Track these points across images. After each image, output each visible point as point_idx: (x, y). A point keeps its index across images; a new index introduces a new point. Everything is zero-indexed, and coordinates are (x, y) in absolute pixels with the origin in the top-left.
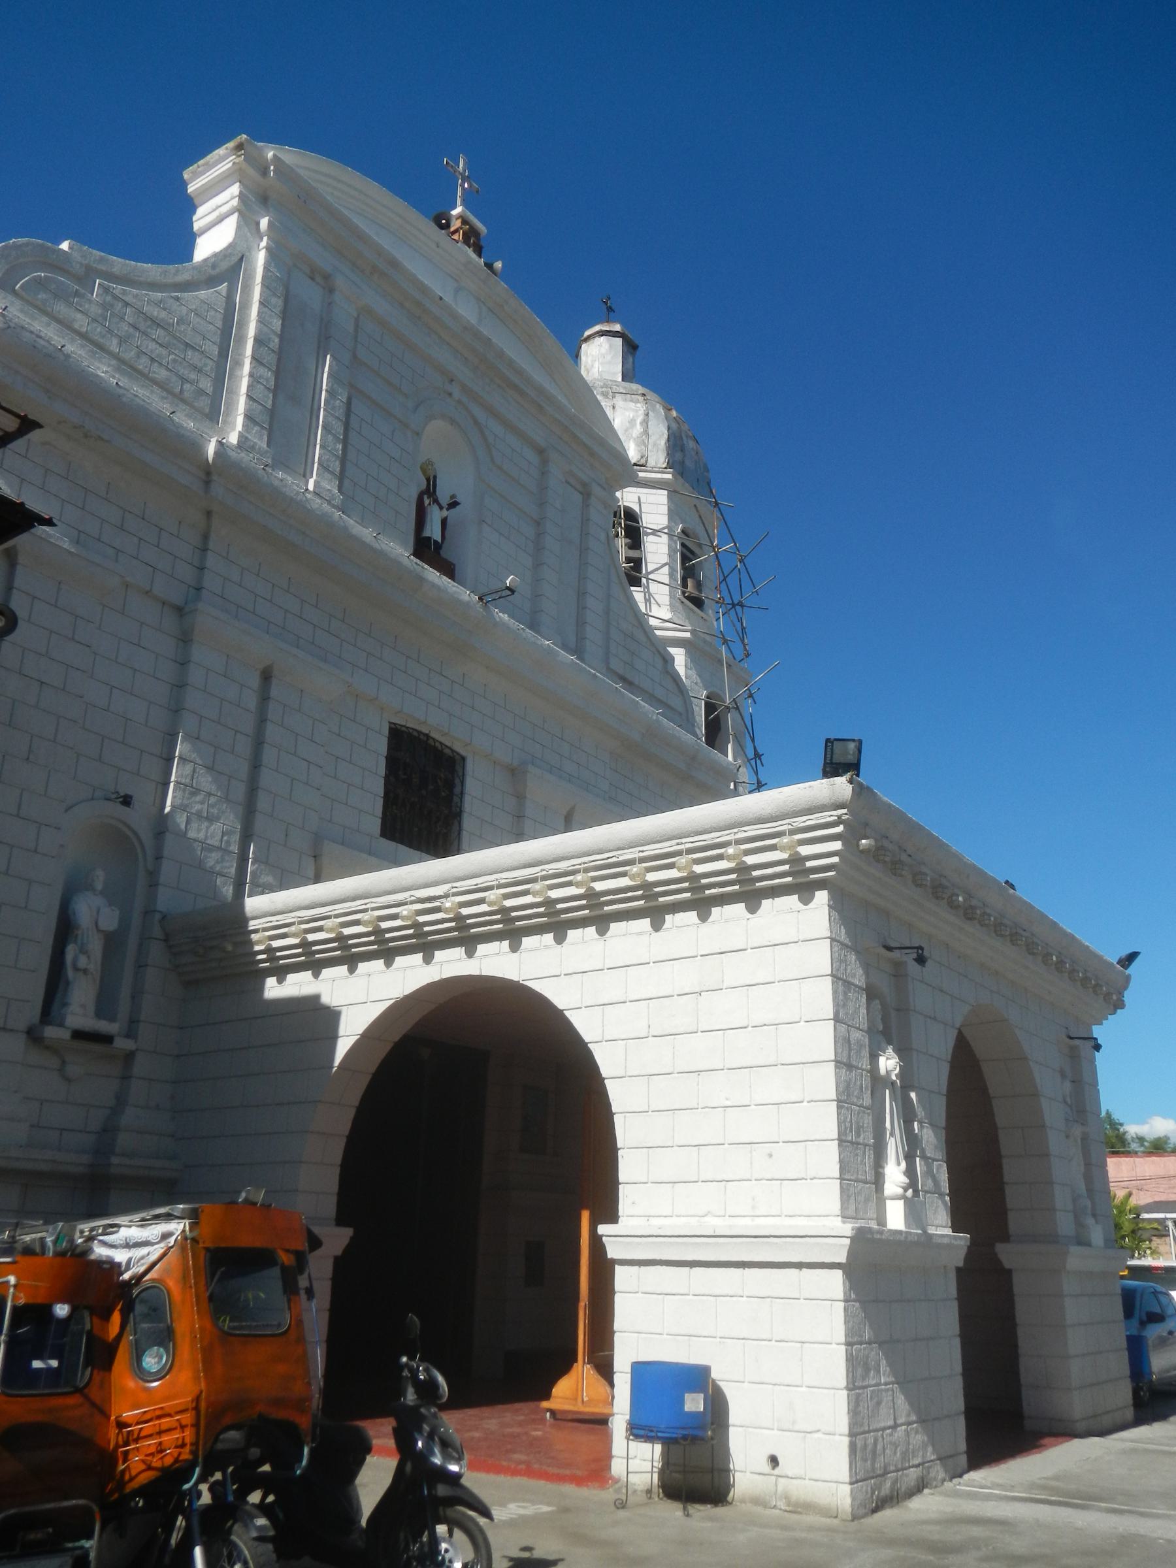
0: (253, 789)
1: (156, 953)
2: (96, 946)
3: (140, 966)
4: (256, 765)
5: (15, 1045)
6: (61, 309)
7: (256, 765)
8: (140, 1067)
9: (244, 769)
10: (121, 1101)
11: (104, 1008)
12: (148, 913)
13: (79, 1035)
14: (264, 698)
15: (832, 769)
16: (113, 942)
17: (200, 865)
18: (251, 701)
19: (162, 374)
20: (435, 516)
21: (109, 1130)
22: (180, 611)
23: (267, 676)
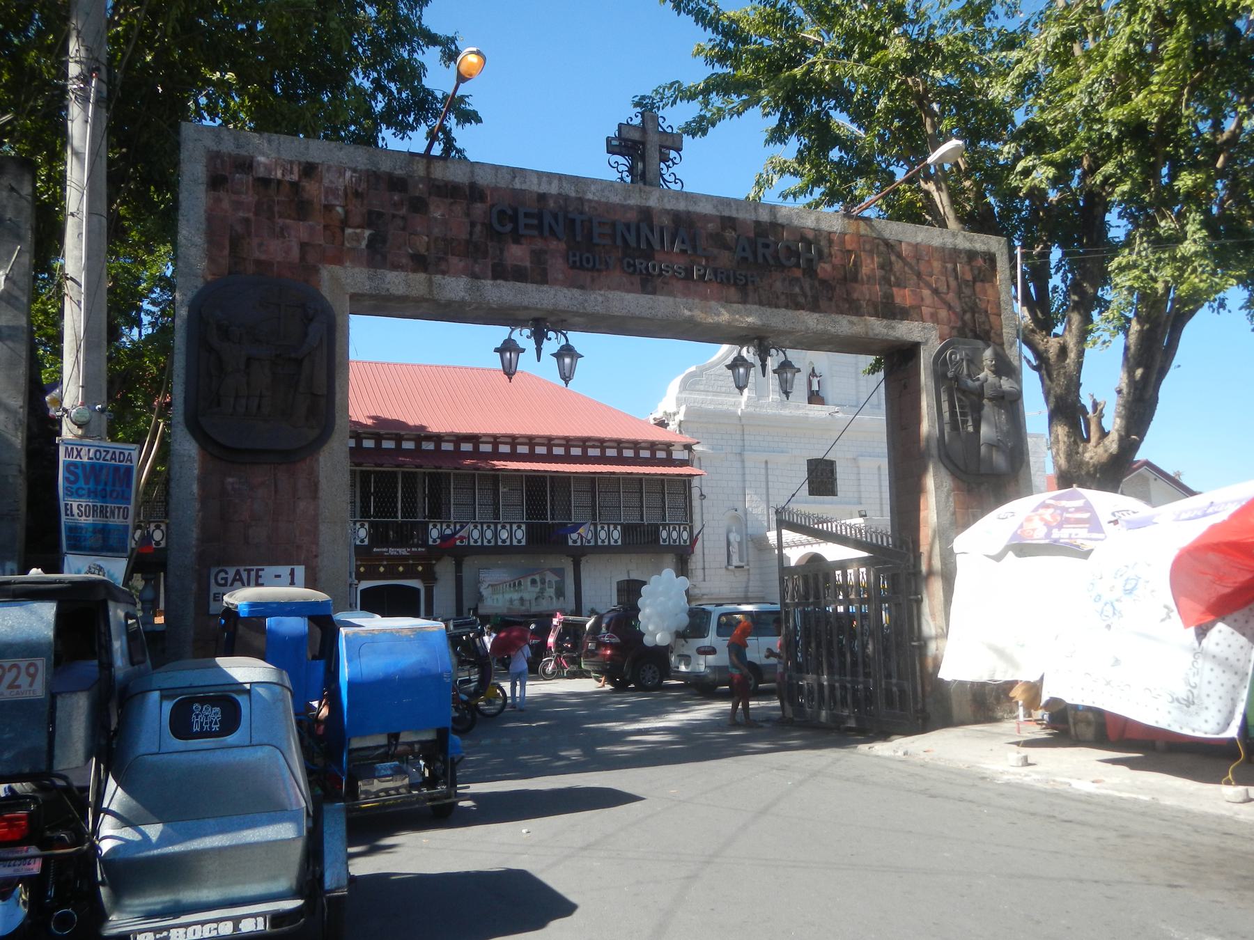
0: (768, 495)
1: (750, 544)
2: (736, 546)
3: (747, 548)
4: (768, 489)
5: (723, 571)
6: (698, 387)
7: (768, 489)
8: (751, 571)
9: (764, 491)
10: (749, 579)
11: (741, 560)
12: (747, 535)
13: (736, 567)
14: (767, 469)
15: (861, 516)
16: (740, 543)
17: (757, 520)
18: (763, 471)
19: (723, 389)
20: (815, 381)
21: (747, 587)
22: (740, 454)
23: (766, 462)
